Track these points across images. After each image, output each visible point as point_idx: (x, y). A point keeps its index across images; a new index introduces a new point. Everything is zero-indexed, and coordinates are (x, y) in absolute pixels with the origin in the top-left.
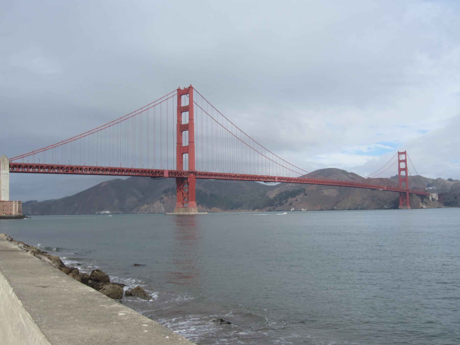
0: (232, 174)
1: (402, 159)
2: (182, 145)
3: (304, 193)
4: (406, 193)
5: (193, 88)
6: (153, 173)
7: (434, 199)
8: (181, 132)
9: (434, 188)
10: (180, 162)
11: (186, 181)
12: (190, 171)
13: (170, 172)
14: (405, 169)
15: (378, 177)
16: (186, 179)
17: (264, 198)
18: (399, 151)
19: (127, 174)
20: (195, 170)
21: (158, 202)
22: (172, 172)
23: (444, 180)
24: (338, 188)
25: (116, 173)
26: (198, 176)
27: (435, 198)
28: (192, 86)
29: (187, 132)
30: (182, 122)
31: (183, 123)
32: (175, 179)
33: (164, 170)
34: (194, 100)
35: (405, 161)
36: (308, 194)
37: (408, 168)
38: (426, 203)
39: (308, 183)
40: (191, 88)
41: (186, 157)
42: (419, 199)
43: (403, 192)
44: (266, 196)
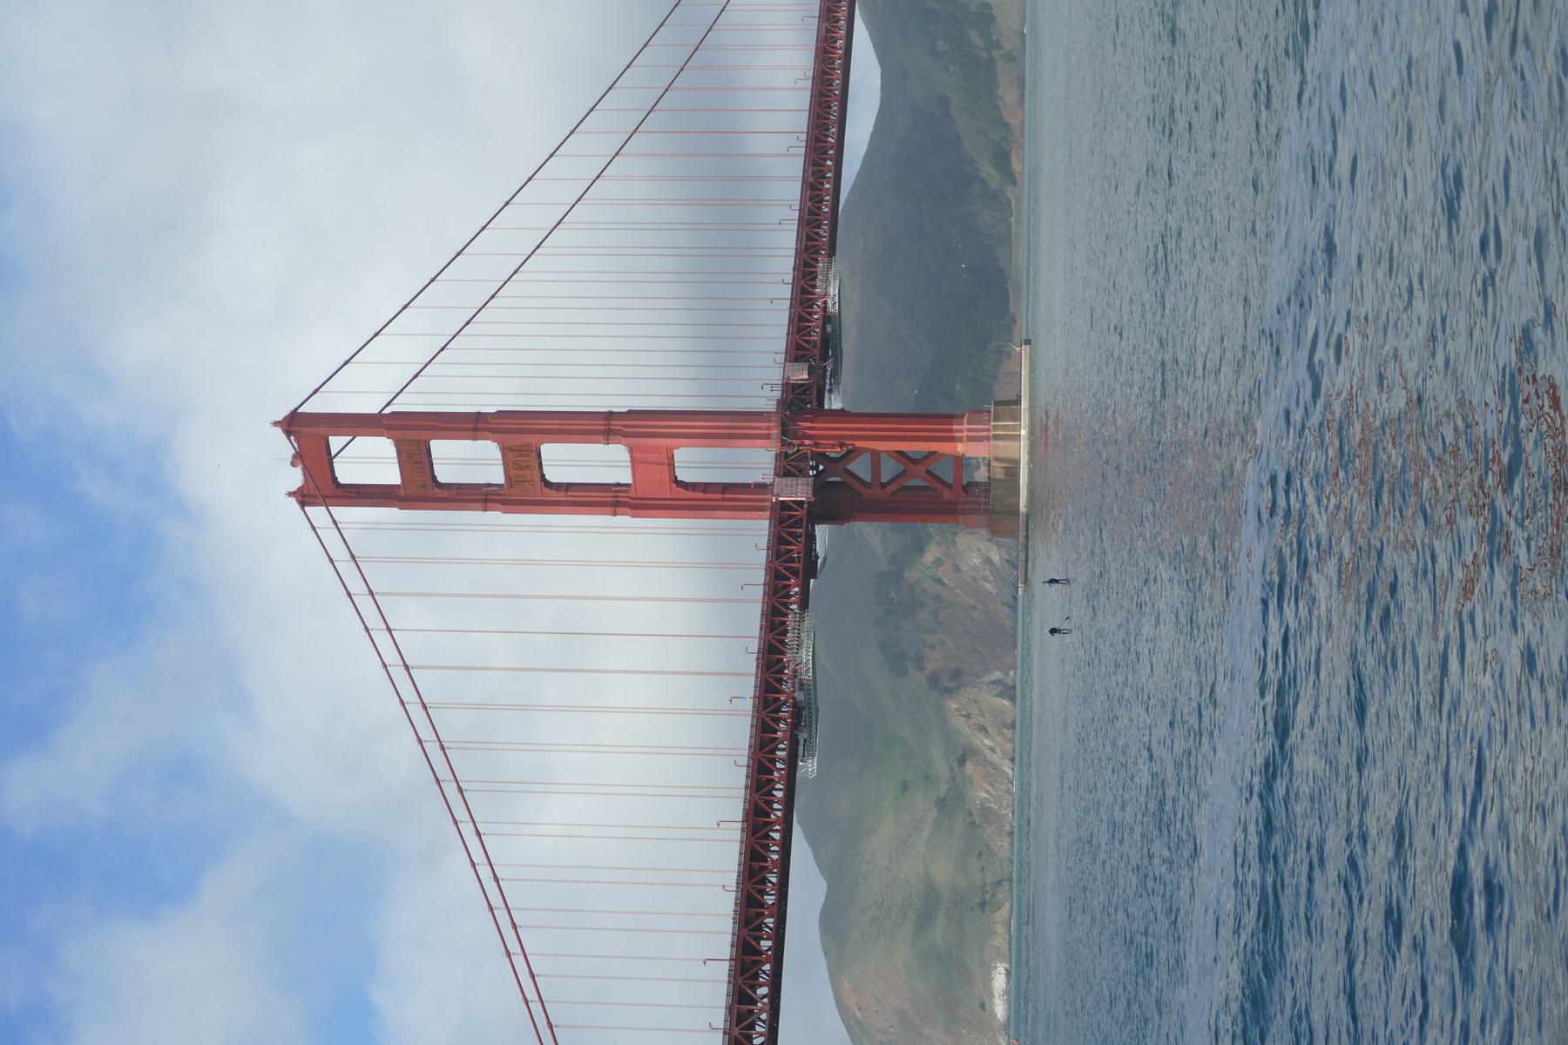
2: (628, 485)
19: (774, 880)
25: (769, 943)
28: (281, 415)
40: (294, 424)
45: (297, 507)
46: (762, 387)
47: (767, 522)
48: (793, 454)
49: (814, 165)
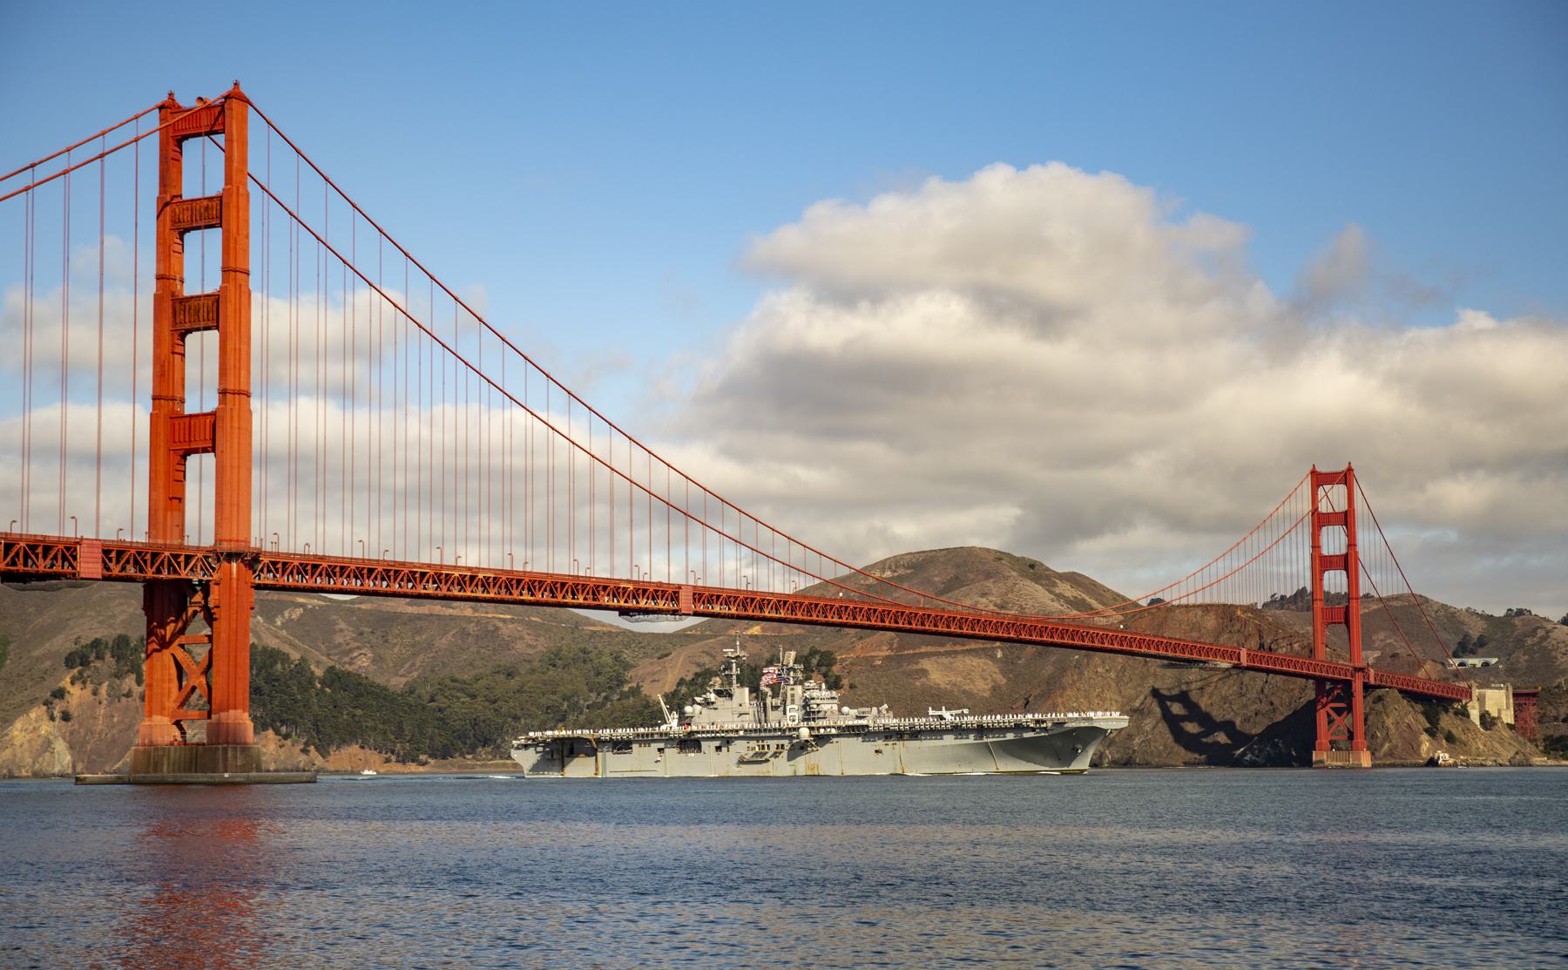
0: (448, 567)
1: (1330, 511)
3: (825, 675)
4: (1348, 684)
5: (248, 102)
6: (17, 554)
7: (1494, 718)
8: (176, 336)
9: (1494, 661)
10: (170, 499)
11: (198, 598)
12: (226, 547)
13: (113, 553)
14: (1347, 562)
15: (1208, 601)
16: (198, 588)
17: (616, 697)
18: (1318, 469)
20: (252, 545)
21: (37, 712)
22: (120, 553)
23: (1544, 619)
24: (999, 655)
26: (268, 578)
27: (1499, 711)
28: (245, 89)
29: (212, 337)
30: (182, 281)
31: (190, 289)
32: (139, 588)
33: (79, 542)
34: (255, 165)
35: (1346, 519)
36: (845, 682)
37: (1361, 556)
38: (1450, 738)
39: (851, 621)
40: (236, 97)
41: (201, 470)
42: (1414, 717)
43: (1335, 681)
44: (626, 689)
45: (159, 102)
46: (275, 534)
47: (141, 537)
48: (209, 564)
49: (495, 578)
